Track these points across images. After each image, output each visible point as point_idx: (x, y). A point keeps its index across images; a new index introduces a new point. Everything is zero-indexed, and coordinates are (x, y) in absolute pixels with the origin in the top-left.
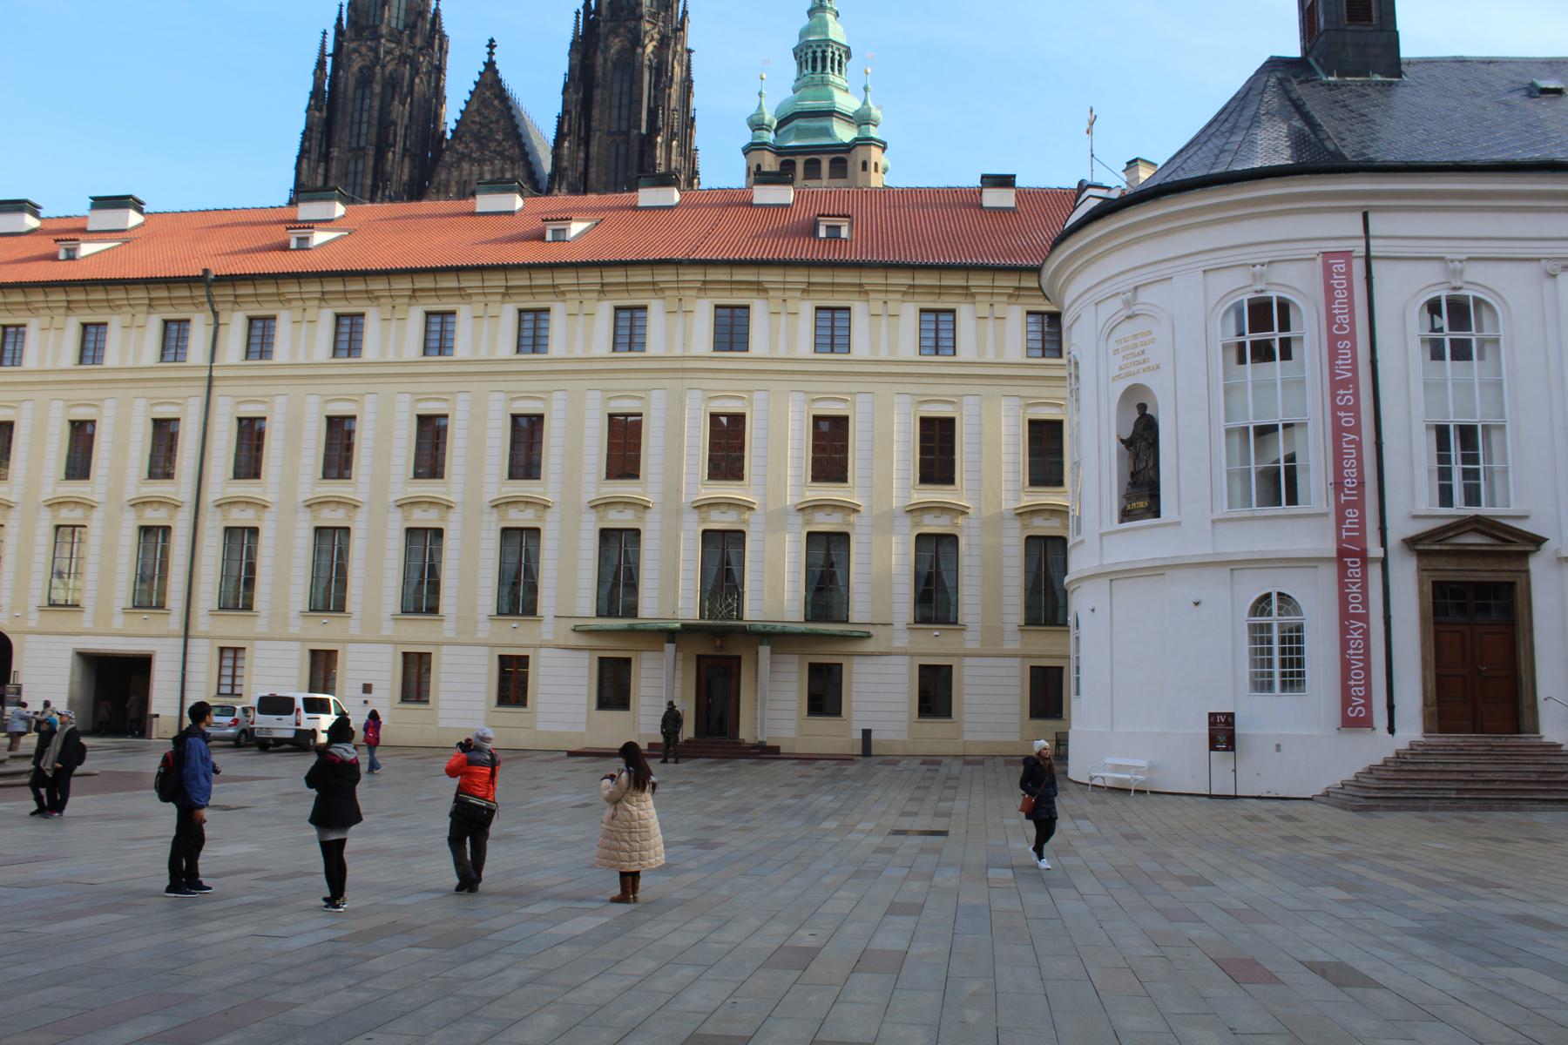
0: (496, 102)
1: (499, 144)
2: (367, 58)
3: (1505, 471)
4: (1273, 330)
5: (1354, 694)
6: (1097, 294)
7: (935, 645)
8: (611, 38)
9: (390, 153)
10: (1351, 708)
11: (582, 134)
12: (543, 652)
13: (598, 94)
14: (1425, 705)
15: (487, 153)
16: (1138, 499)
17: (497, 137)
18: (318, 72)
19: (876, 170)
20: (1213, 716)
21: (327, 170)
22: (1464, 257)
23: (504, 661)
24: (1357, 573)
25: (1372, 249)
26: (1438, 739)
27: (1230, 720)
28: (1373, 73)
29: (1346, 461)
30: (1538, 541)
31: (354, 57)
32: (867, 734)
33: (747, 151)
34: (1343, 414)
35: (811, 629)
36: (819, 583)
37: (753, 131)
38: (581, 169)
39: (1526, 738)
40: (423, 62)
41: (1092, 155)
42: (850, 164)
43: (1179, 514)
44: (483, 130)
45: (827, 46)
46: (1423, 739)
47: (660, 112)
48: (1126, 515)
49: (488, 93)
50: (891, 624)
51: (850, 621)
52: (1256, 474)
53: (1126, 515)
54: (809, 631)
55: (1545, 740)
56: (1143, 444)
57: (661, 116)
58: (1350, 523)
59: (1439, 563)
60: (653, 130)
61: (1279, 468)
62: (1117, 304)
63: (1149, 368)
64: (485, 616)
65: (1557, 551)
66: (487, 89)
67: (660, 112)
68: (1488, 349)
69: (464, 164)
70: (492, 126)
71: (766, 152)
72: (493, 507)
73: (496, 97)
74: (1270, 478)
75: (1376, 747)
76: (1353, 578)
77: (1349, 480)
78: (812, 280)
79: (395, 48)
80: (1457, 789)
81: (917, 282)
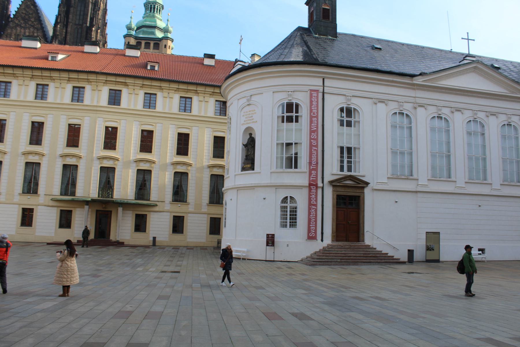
3: (359, 162)
4: (293, 113)
5: (311, 229)
6: (238, 96)
7: (179, 209)
10: (310, 233)
12: (39, 207)
13: (72, 10)
14: (332, 233)
16: (248, 164)
19: (169, 48)
20: (268, 235)
22: (351, 95)
23: (24, 210)
24: (314, 191)
25: (325, 90)
26: (336, 243)
27: (273, 236)
28: (329, 36)
29: (313, 156)
30: (367, 184)
32: (154, 238)
33: (125, 37)
34: (313, 141)
35: (137, 202)
36: (140, 187)
37: (128, 30)
38: (64, 36)
41: (240, 51)
42: (160, 45)
43: (260, 170)
45: (156, 4)
46: (331, 243)
47: (95, 19)
48: (243, 169)
50: (164, 202)
51: (150, 200)
52: (285, 158)
53: (243, 169)
55: (366, 244)
56: (250, 146)
57: (95, 21)
58: (313, 175)
59: (339, 189)
60: (92, 25)
61: (292, 157)
62: (244, 100)
63: (253, 122)
64: (17, 194)
65: (372, 187)
67: (95, 19)
68: (357, 124)
71: (132, 38)
72: (23, 154)
74: (289, 159)
75: (317, 246)
76: (313, 193)
77: (314, 162)
78: (144, 83)
80: (341, 259)
81: (180, 87)
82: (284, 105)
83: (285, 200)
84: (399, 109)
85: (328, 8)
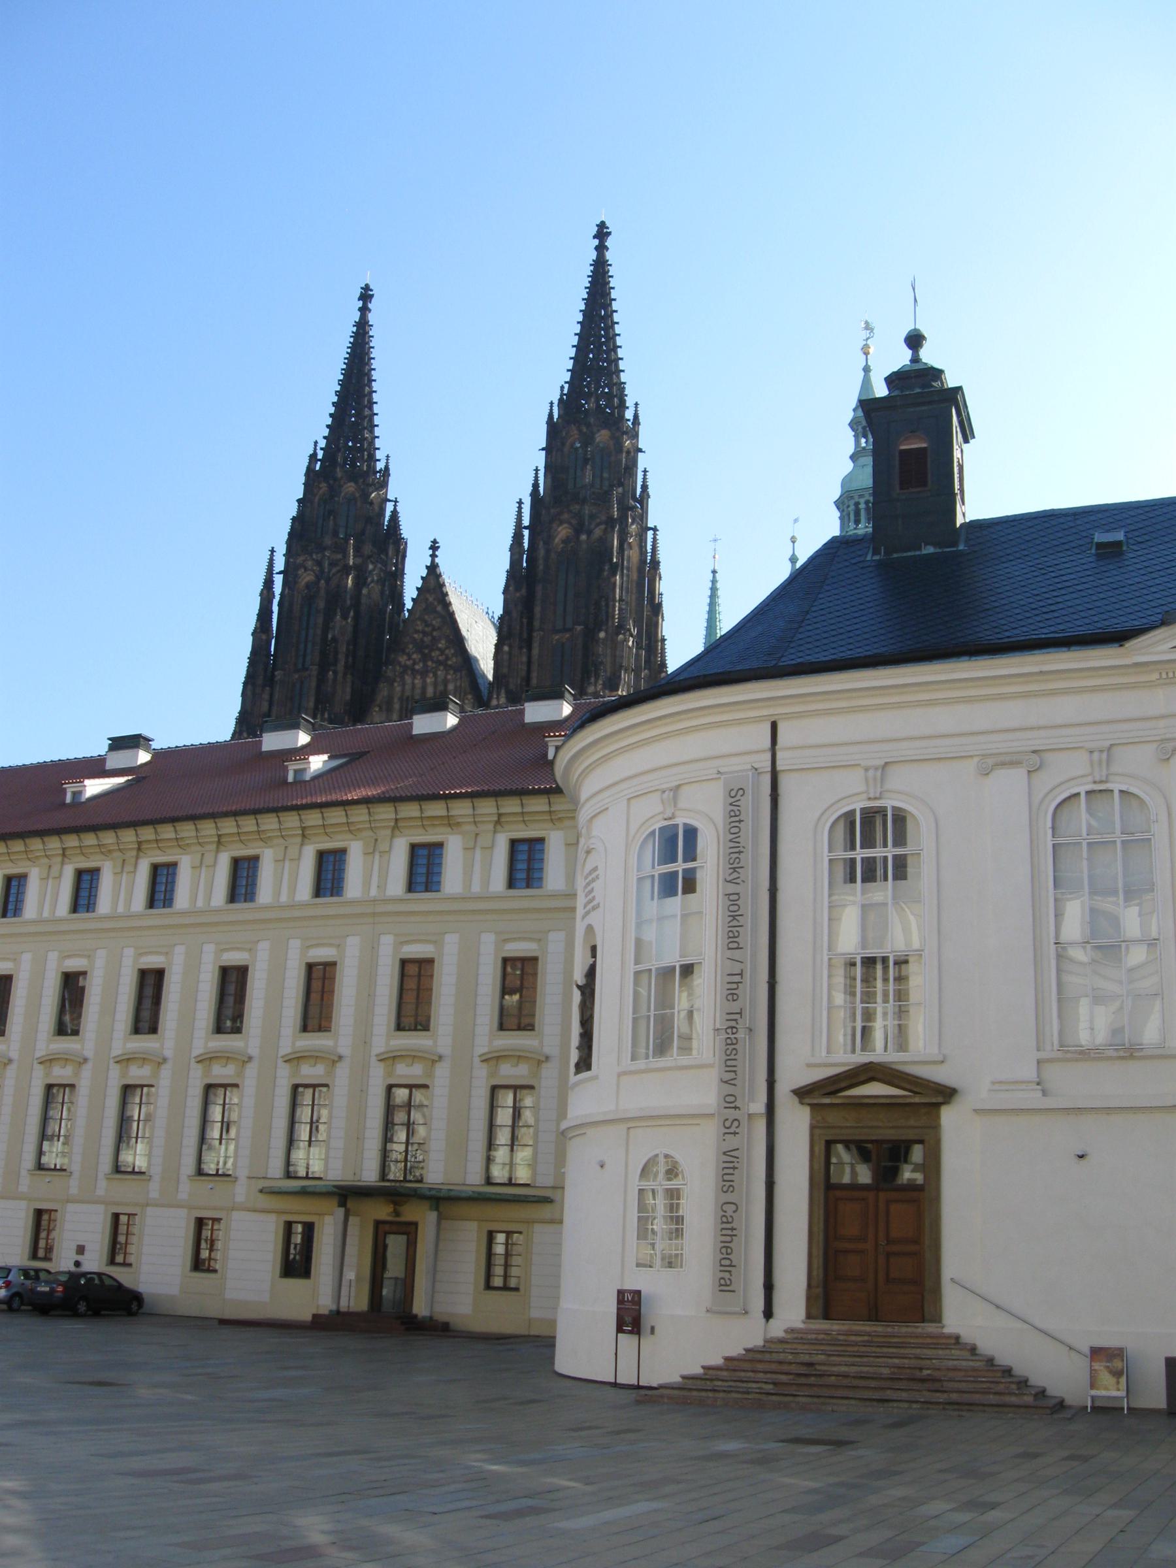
1: (442, 652)
8: (554, 525)
9: (331, 673)
11: (525, 636)
12: (236, 1215)
13: (539, 589)
14: (809, 1286)
15: (430, 663)
17: (440, 645)
18: (265, 592)
20: (620, 1293)
21: (271, 695)
25: (778, 763)
27: (636, 1299)
28: (925, 545)
30: (948, 1094)
31: (300, 572)
38: (524, 673)
40: (374, 570)
44: (425, 639)
55: (946, 1330)
57: (604, 608)
59: (833, 1118)
67: (603, 604)
69: (406, 677)
70: (435, 634)
79: (340, 560)
82: (676, 836)
85: (924, 445)
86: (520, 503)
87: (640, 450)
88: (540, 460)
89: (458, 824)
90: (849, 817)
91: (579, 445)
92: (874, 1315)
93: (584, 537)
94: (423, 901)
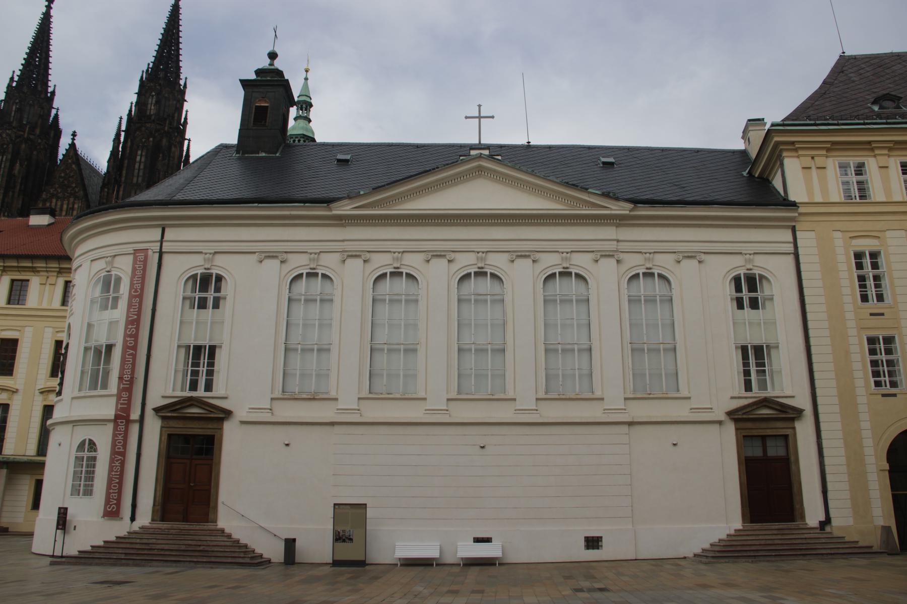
0: (74, 166)
2: (5, 139)
5: (112, 498)
10: (109, 506)
14: (154, 505)
24: (122, 428)
25: (163, 248)
28: (262, 152)
29: (126, 365)
30: (228, 414)
34: (129, 339)
35: (31, 460)
39: (207, 525)
46: (149, 525)
49: (70, 161)
54: (29, 461)
55: (218, 527)
58: (123, 400)
59: (172, 423)
66: (70, 159)
73: (73, 163)
75: (120, 528)
76: (120, 431)
77: (126, 376)
78: (7, 264)
80: (125, 554)
83: (81, 447)
84: (309, 267)
85: (267, 105)
86: (121, 118)
87: (186, 101)
88: (134, 98)
89: (39, 272)
90: (194, 277)
91: (154, 94)
92: (186, 519)
93: (151, 139)
94: (15, 309)
